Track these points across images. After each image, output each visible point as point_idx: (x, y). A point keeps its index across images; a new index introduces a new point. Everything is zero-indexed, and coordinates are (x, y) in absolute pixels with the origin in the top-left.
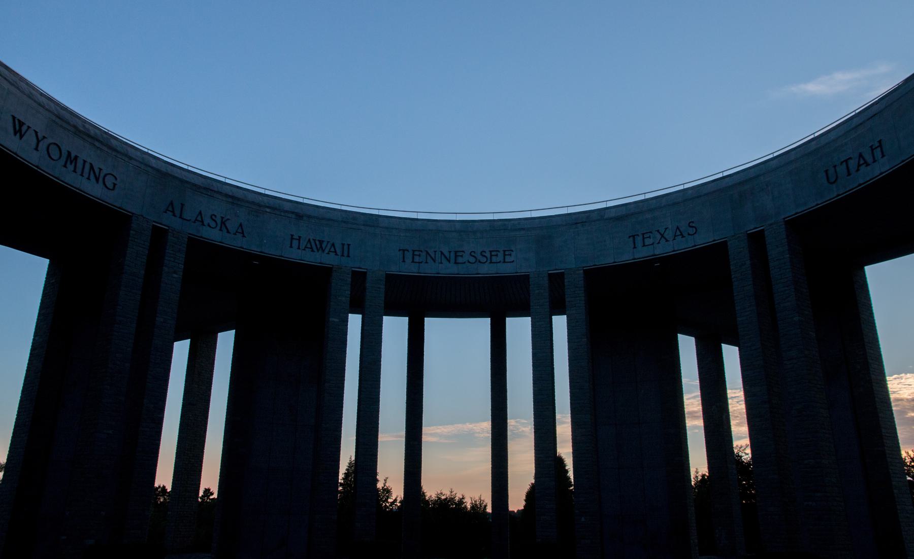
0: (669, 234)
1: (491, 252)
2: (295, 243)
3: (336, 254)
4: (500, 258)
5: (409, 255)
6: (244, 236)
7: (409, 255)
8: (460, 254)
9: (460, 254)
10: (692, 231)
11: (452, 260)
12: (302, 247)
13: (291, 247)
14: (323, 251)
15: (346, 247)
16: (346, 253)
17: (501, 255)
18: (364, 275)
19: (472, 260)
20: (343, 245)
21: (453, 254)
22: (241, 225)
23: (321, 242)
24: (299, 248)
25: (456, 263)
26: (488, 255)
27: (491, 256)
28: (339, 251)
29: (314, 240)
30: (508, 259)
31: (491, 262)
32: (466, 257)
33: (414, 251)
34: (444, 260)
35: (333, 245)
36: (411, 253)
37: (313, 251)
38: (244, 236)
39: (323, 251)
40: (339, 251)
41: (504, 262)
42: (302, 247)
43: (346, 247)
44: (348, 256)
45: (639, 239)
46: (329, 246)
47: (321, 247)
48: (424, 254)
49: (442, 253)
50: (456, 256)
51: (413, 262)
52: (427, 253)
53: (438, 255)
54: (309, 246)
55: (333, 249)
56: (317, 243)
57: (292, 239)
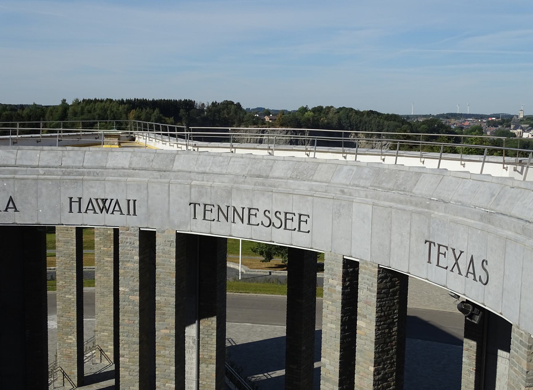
1: (286, 213)
2: (75, 206)
3: (122, 214)
4: (295, 225)
5: (200, 209)
6: (16, 210)
7: (200, 209)
13: (71, 211)
15: (131, 203)
17: (296, 218)
21: (246, 212)
22: (11, 199)
23: (104, 201)
24: (80, 211)
25: (249, 223)
26: (282, 217)
27: (286, 219)
28: (125, 211)
31: (285, 228)
32: (261, 217)
33: (205, 205)
35: (117, 202)
36: (202, 206)
37: (95, 212)
38: (16, 210)
40: (125, 211)
41: (299, 230)
42: (83, 209)
43: (131, 203)
44: (135, 214)
47: (104, 206)
48: (215, 209)
50: (250, 215)
51: (204, 219)
52: (219, 208)
54: (90, 207)
55: (117, 208)
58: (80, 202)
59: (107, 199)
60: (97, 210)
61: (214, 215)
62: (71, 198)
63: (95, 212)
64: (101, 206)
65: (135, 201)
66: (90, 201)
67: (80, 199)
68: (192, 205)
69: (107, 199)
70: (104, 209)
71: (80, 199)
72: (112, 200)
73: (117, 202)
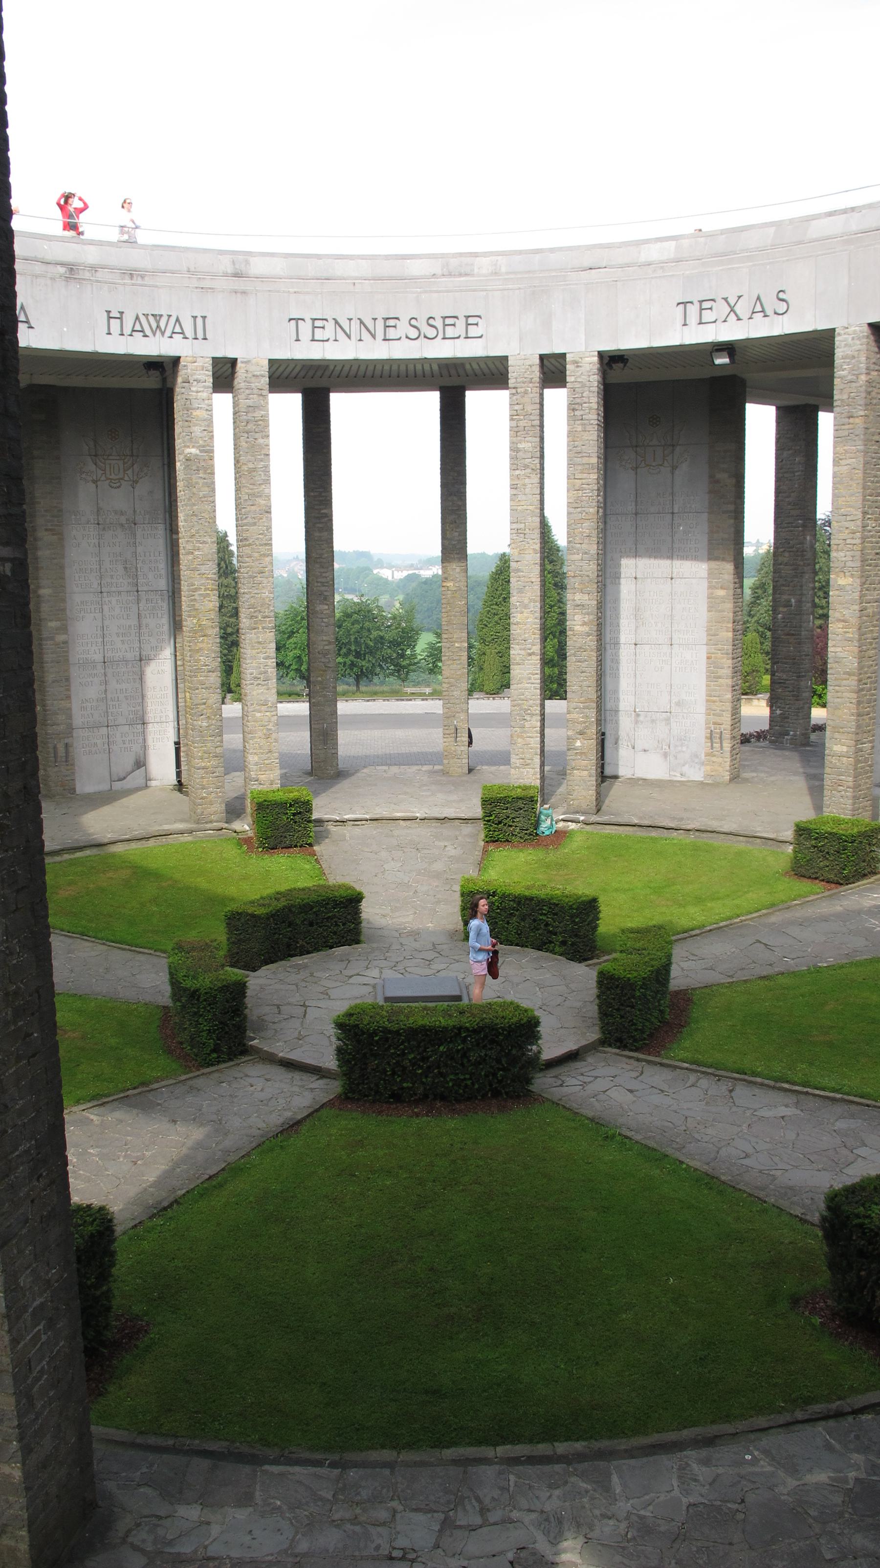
0: (742, 308)
1: (444, 318)
4: (460, 329)
7: (305, 328)
8: (391, 323)
9: (391, 323)
10: (782, 307)
11: (380, 334)
12: (127, 330)
14: (163, 333)
15: (199, 321)
16: (200, 335)
17: (461, 324)
18: (233, 362)
19: (413, 333)
20: (195, 318)
21: (380, 324)
23: (157, 317)
26: (438, 323)
27: (445, 325)
28: (189, 333)
29: (146, 315)
30: (473, 331)
31: (444, 338)
32: (403, 328)
34: (365, 335)
35: (178, 320)
36: (309, 322)
39: (163, 333)
40: (189, 333)
43: (199, 321)
45: (693, 310)
46: (173, 320)
47: (158, 327)
49: (362, 322)
53: (355, 324)
55: (178, 329)
56: (151, 319)
57: (110, 318)
58: (121, 318)
59: (161, 316)
60: (148, 332)
61: (329, 331)
62: (109, 312)
63: (145, 336)
64: (154, 325)
65: (204, 318)
66: (137, 318)
67: (122, 313)
68: (293, 323)
69: (161, 316)
70: (158, 330)
71: (122, 313)
72: (170, 316)
73: (178, 320)
